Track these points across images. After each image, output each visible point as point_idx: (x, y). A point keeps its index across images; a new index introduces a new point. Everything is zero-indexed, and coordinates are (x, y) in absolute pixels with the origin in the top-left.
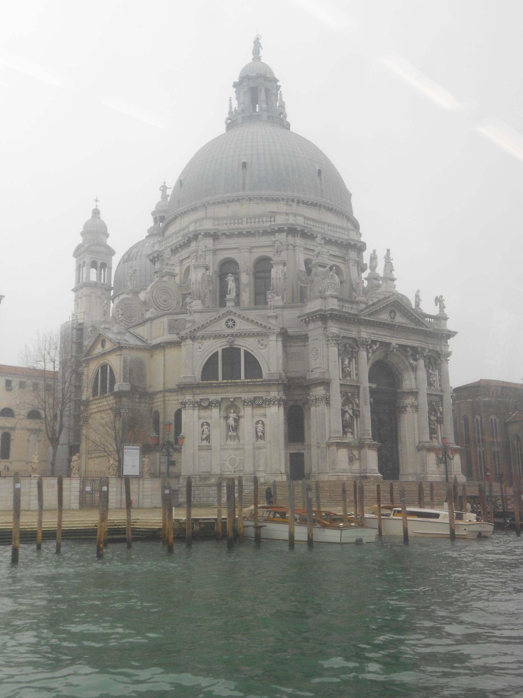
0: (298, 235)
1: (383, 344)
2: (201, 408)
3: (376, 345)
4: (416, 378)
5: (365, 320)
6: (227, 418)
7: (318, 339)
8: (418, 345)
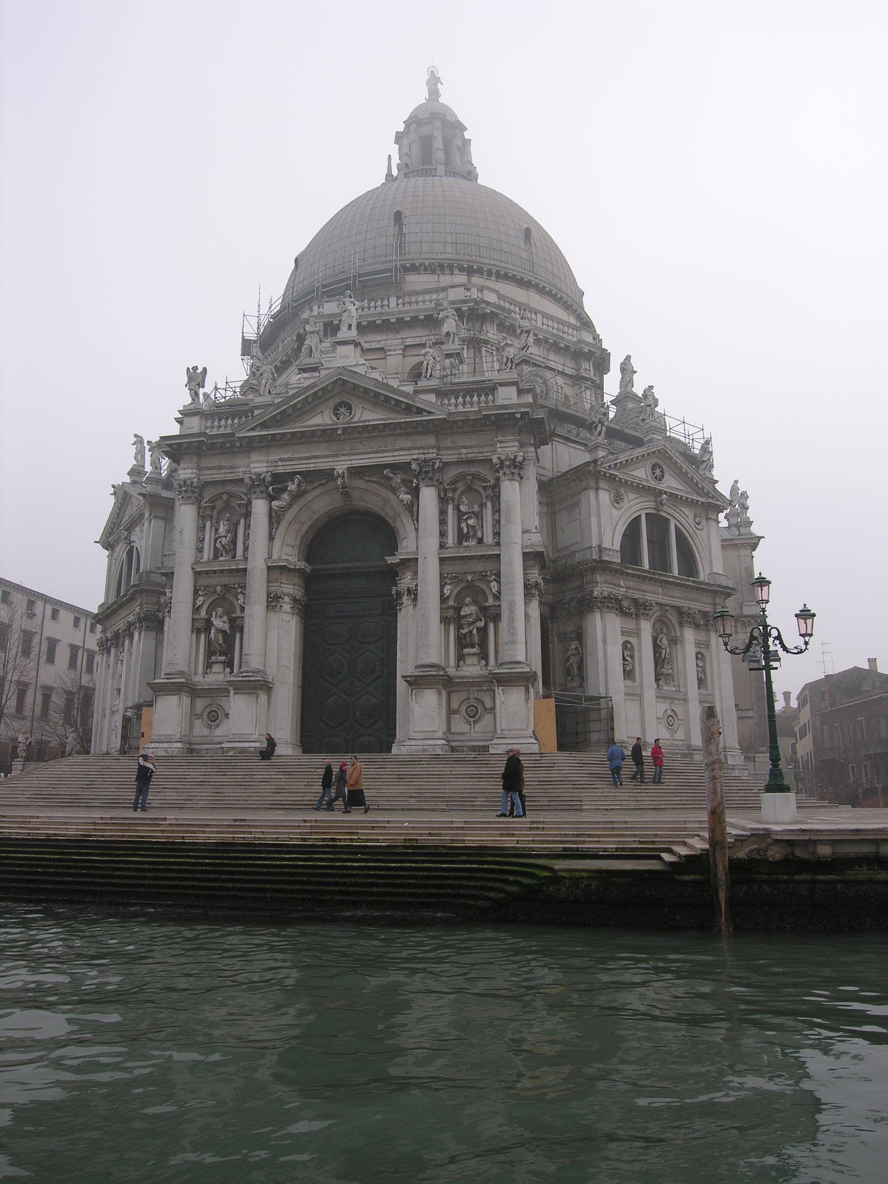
1: (309, 476)
8: (415, 457)
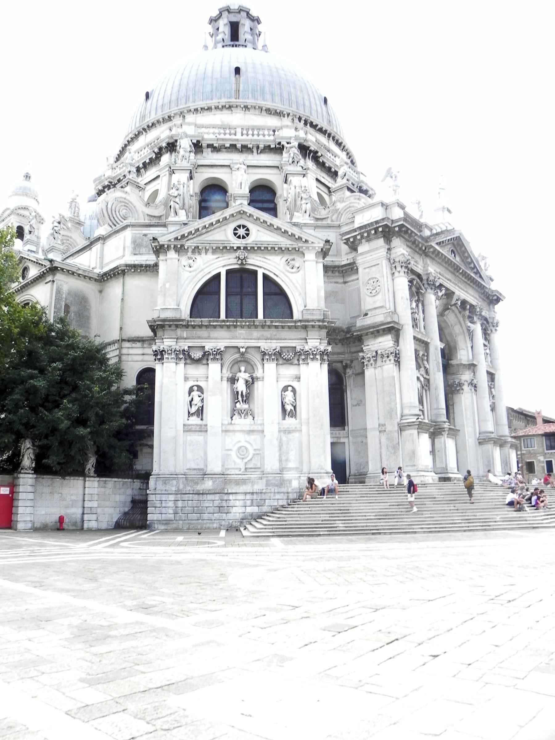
0: (309, 157)
2: (188, 361)
3: (441, 291)
4: (472, 347)
5: (435, 250)
6: (233, 380)
7: (378, 264)
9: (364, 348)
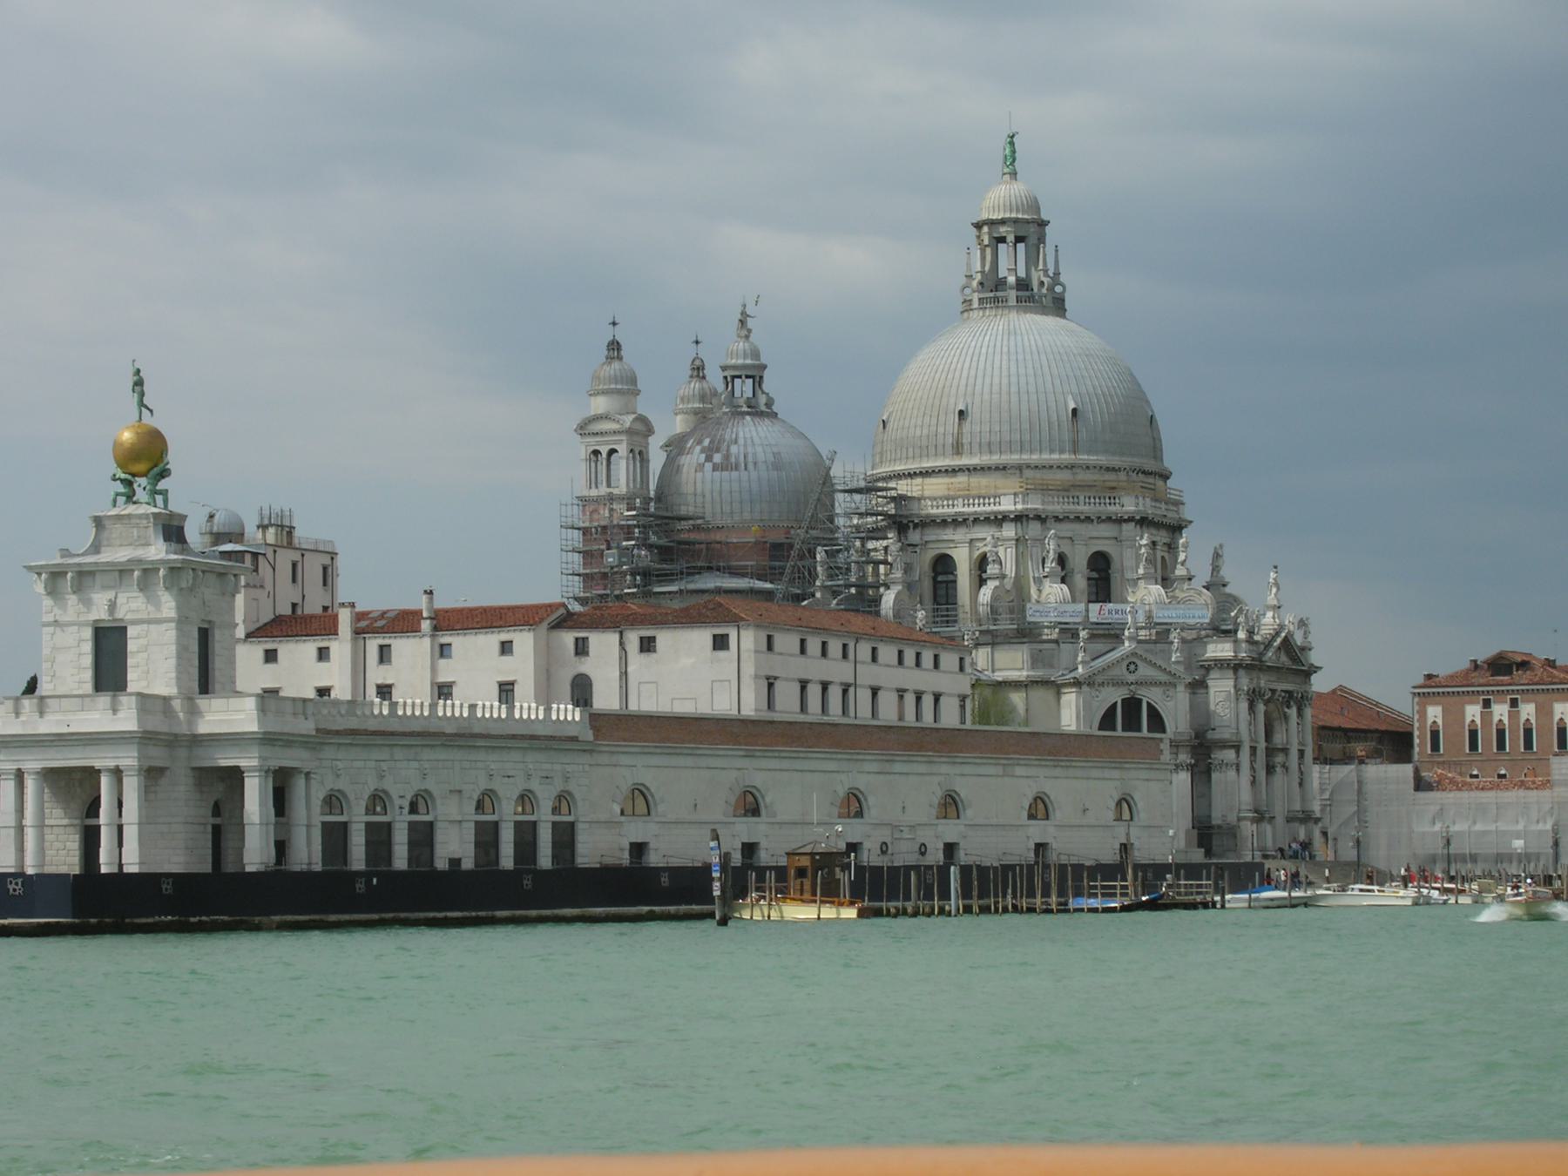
4: (1287, 730)
5: (1268, 666)
9: (1212, 756)
